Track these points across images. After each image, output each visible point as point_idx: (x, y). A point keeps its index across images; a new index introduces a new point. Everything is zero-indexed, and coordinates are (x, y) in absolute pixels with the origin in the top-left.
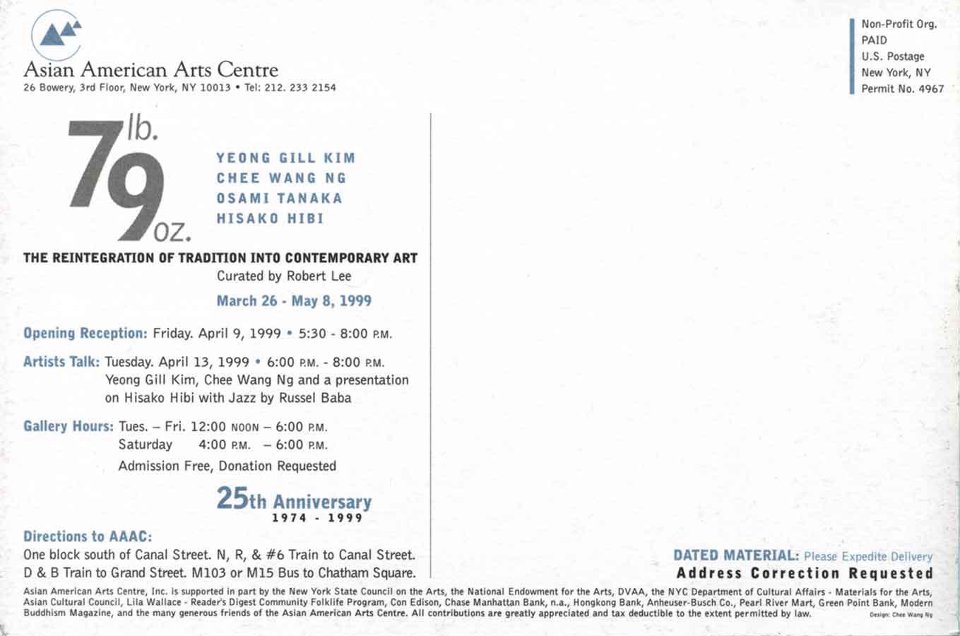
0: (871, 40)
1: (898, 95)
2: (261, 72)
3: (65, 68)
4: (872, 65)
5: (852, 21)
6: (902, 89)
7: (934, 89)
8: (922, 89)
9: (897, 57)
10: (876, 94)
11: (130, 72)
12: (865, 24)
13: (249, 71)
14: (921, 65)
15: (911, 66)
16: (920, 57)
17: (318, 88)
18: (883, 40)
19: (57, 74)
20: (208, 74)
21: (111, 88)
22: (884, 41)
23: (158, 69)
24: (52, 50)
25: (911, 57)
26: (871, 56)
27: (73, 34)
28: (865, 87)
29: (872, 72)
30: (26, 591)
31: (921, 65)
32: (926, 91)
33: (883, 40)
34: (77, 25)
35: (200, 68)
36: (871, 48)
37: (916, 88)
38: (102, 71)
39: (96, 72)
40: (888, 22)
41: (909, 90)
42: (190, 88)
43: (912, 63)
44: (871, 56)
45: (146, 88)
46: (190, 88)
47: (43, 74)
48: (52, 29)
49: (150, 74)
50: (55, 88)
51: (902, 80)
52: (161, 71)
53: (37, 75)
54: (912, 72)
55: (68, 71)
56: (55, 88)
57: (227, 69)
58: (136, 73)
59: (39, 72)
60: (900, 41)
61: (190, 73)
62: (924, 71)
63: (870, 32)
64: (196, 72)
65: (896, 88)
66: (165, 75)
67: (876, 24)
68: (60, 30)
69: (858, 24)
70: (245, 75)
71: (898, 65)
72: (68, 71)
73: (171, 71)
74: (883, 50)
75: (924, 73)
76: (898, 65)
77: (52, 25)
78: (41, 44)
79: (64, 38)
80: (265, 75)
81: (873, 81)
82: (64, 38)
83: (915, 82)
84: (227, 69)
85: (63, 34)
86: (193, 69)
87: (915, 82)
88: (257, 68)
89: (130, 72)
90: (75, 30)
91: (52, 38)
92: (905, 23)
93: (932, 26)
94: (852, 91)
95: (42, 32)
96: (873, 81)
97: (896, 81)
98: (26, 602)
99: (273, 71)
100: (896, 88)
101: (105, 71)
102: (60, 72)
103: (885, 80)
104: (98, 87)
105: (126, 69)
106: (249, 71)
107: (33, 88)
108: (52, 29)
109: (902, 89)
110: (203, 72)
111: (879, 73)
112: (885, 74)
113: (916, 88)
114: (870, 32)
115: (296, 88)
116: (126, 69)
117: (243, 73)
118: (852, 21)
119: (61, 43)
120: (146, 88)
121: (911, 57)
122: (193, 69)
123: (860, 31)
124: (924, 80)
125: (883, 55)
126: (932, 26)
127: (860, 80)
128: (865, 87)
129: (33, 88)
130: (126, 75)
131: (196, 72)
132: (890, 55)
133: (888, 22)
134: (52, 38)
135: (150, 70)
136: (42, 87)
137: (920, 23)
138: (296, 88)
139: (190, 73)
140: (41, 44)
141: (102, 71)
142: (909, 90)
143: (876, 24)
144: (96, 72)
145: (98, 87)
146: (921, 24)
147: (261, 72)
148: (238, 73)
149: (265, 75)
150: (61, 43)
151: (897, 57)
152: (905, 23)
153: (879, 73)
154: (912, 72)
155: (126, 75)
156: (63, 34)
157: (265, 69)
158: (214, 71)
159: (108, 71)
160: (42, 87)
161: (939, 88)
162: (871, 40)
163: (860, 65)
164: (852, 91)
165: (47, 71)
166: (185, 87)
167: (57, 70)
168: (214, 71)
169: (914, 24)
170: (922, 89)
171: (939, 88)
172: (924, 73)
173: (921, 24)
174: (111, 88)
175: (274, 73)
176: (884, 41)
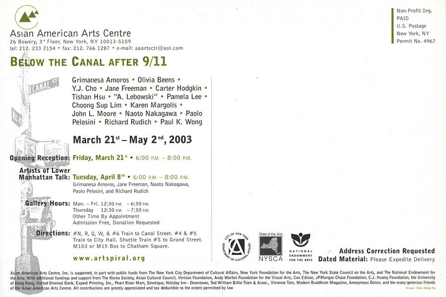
0: (401, 18)
1: (414, 44)
4: (401, 30)
5: (392, 9)
6: (416, 41)
7: (431, 41)
8: (425, 41)
9: (414, 26)
10: (404, 44)
14: (424, 30)
15: (420, 30)
16: (424, 26)
18: (407, 18)
22: (407, 18)
25: (420, 26)
26: (401, 26)
31: (424, 30)
33: (407, 18)
36: (401, 22)
37: (422, 40)
40: (409, 10)
41: (419, 42)
44: (401, 26)
51: (416, 37)
54: (421, 33)
60: (415, 19)
62: (426, 33)
63: (400, 15)
65: (413, 41)
69: (395, 11)
71: (414, 30)
74: (407, 23)
75: (426, 34)
76: (414, 30)
81: (402, 38)
87: (422, 38)
93: (430, 11)
94: (393, 42)
96: (402, 38)
100: (413, 41)
109: (416, 41)
111: (405, 34)
112: (408, 34)
113: (422, 40)
114: (400, 15)
118: (392, 9)
121: (420, 26)
123: (396, 14)
124: (426, 37)
126: (430, 11)
127: (396, 37)
132: (410, 25)
142: (419, 42)
146: (425, 11)
151: (414, 26)
153: (405, 34)
154: (421, 33)
161: (433, 41)
163: (396, 30)
164: (393, 42)
170: (425, 41)
171: (433, 41)
172: (426, 34)
173: (425, 11)
176: (407, 18)
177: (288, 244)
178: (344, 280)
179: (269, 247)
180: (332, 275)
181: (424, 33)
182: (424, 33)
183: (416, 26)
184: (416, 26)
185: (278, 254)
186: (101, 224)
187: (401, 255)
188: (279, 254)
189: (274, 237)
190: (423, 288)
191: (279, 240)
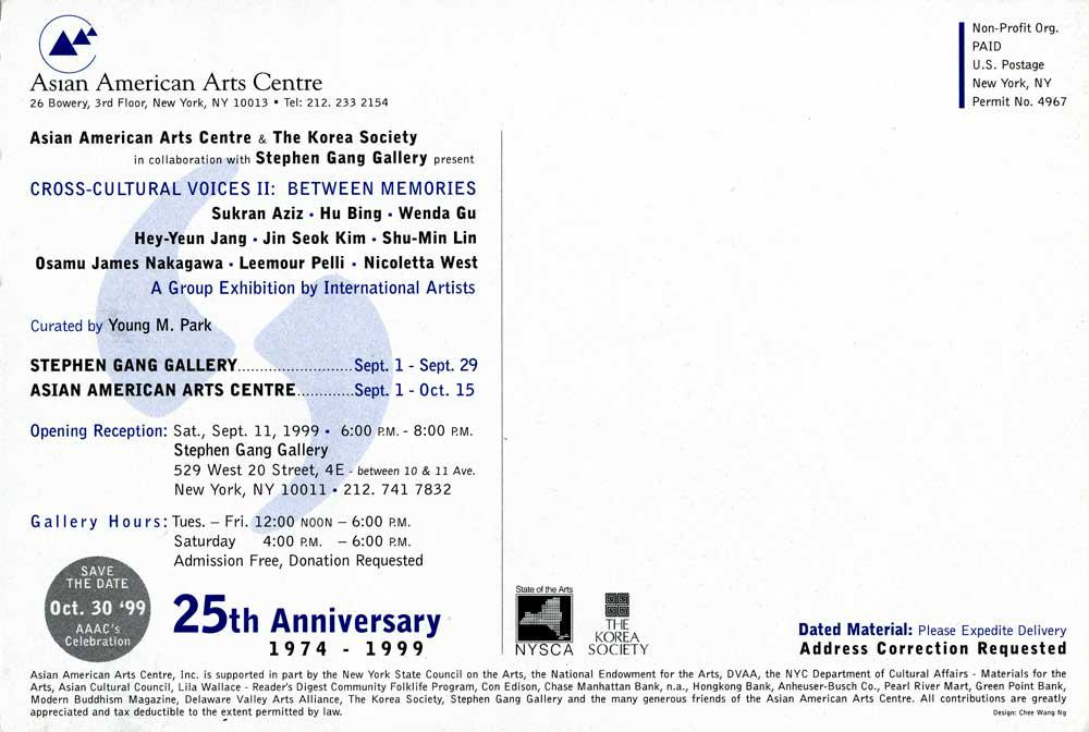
0: (983, 46)
2: (303, 84)
3: (78, 82)
4: (984, 75)
5: (962, 26)
7: (1056, 102)
8: (1041, 101)
9: (1013, 66)
11: (152, 85)
12: (976, 27)
13: (289, 84)
14: (1040, 74)
15: (1029, 76)
16: (1039, 66)
17: (368, 103)
18: (996, 46)
19: (69, 88)
20: (242, 88)
21: (131, 104)
23: (185, 81)
24: (62, 61)
25: (1029, 66)
26: (983, 64)
27: (88, 43)
28: (975, 100)
29: (984, 82)
30: (34, 675)
31: (1040, 74)
32: (1046, 103)
33: (996, 46)
34: (92, 33)
35: (233, 80)
36: (983, 55)
37: (1034, 100)
38: (121, 84)
39: (114, 86)
40: (1003, 26)
42: (221, 103)
43: (1031, 71)
44: (983, 64)
45: (172, 104)
46: (221, 103)
47: (53, 88)
48: (63, 36)
49: (176, 88)
50: (66, 104)
52: (189, 85)
53: (45, 89)
54: (1030, 82)
55: (82, 85)
56: (66, 104)
57: (264, 82)
58: (159, 86)
59: (48, 86)
60: (1017, 47)
61: (221, 86)
64: (229, 85)
65: (1012, 102)
66: (193, 89)
67: (990, 28)
68: (72, 38)
69: (968, 29)
70: (285, 89)
71: (1015, 75)
72: (82, 85)
73: (199, 85)
74: (996, 57)
76: (1015, 75)
77: (63, 33)
78: (51, 54)
79: (77, 47)
80: (307, 89)
82: (75, 47)
83: (1034, 94)
84: (264, 82)
85: (75, 43)
86: (224, 81)
87: (1034, 94)
88: (298, 80)
89: (152, 85)
90: (89, 38)
91: (63, 47)
92: (1022, 27)
93: (1053, 30)
94: (962, 105)
95: (51, 41)
97: (1012, 93)
98: (34, 687)
99: (315, 84)
100: (1012, 102)
101: (123, 84)
102: (74, 86)
103: (999, 92)
104: (115, 102)
105: (148, 82)
106: (289, 84)
107: (40, 104)
108: (63, 36)
110: (236, 85)
111: (992, 84)
112: (1000, 84)
113: (1034, 100)
115: (343, 103)
116: (148, 82)
117: (282, 86)
118: (962, 26)
119: (74, 53)
120: (172, 104)
121: (1029, 66)
122: (224, 81)
124: (1045, 92)
125: (997, 62)
126: (1053, 30)
127: (970, 92)
128: (975, 100)
129: (40, 104)
130: (148, 89)
131: (229, 85)
133: (1003, 26)
134: (63, 47)
135: (176, 83)
136: (52, 103)
137: (1039, 26)
138: (343, 103)
139: (221, 86)
140: (51, 54)
141: (121, 84)
143: (990, 28)
144: (114, 86)
145: (115, 102)
146: (1040, 28)
147: (303, 84)
148: (276, 86)
149: (307, 89)
150: (74, 53)
152: (1022, 27)
153: (992, 84)
154: (1030, 82)
155: (148, 89)
156: (75, 43)
157: (307, 81)
158: (249, 84)
159: (128, 84)
160: (52, 103)
161: (1061, 101)
162: (983, 46)
163: (970, 74)
164: (962, 105)
165: (58, 85)
166: (215, 102)
167: (69, 83)
168: (249, 84)
169: (1033, 28)
170: (1041, 101)
171: (1061, 101)
173: (1040, 28)
174: (131, 104)
175: (317, 86)
177: (588, 617)
178: (904, 693)
179: (541, 622)
180: (820, 681)
181: (1038, 83)
182: (1038, 83)
183: (1022, 65)
184: (1022, 65)
185: (562, 637)
186: (256, 563)
187: (844, 639)
188: (565, 639)
189: (551, 597)
190: (1036, 713)
191: (566, 603)
